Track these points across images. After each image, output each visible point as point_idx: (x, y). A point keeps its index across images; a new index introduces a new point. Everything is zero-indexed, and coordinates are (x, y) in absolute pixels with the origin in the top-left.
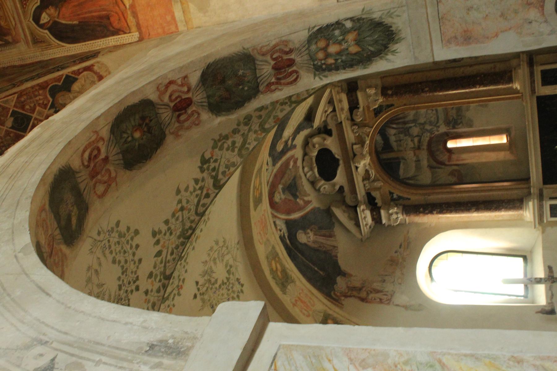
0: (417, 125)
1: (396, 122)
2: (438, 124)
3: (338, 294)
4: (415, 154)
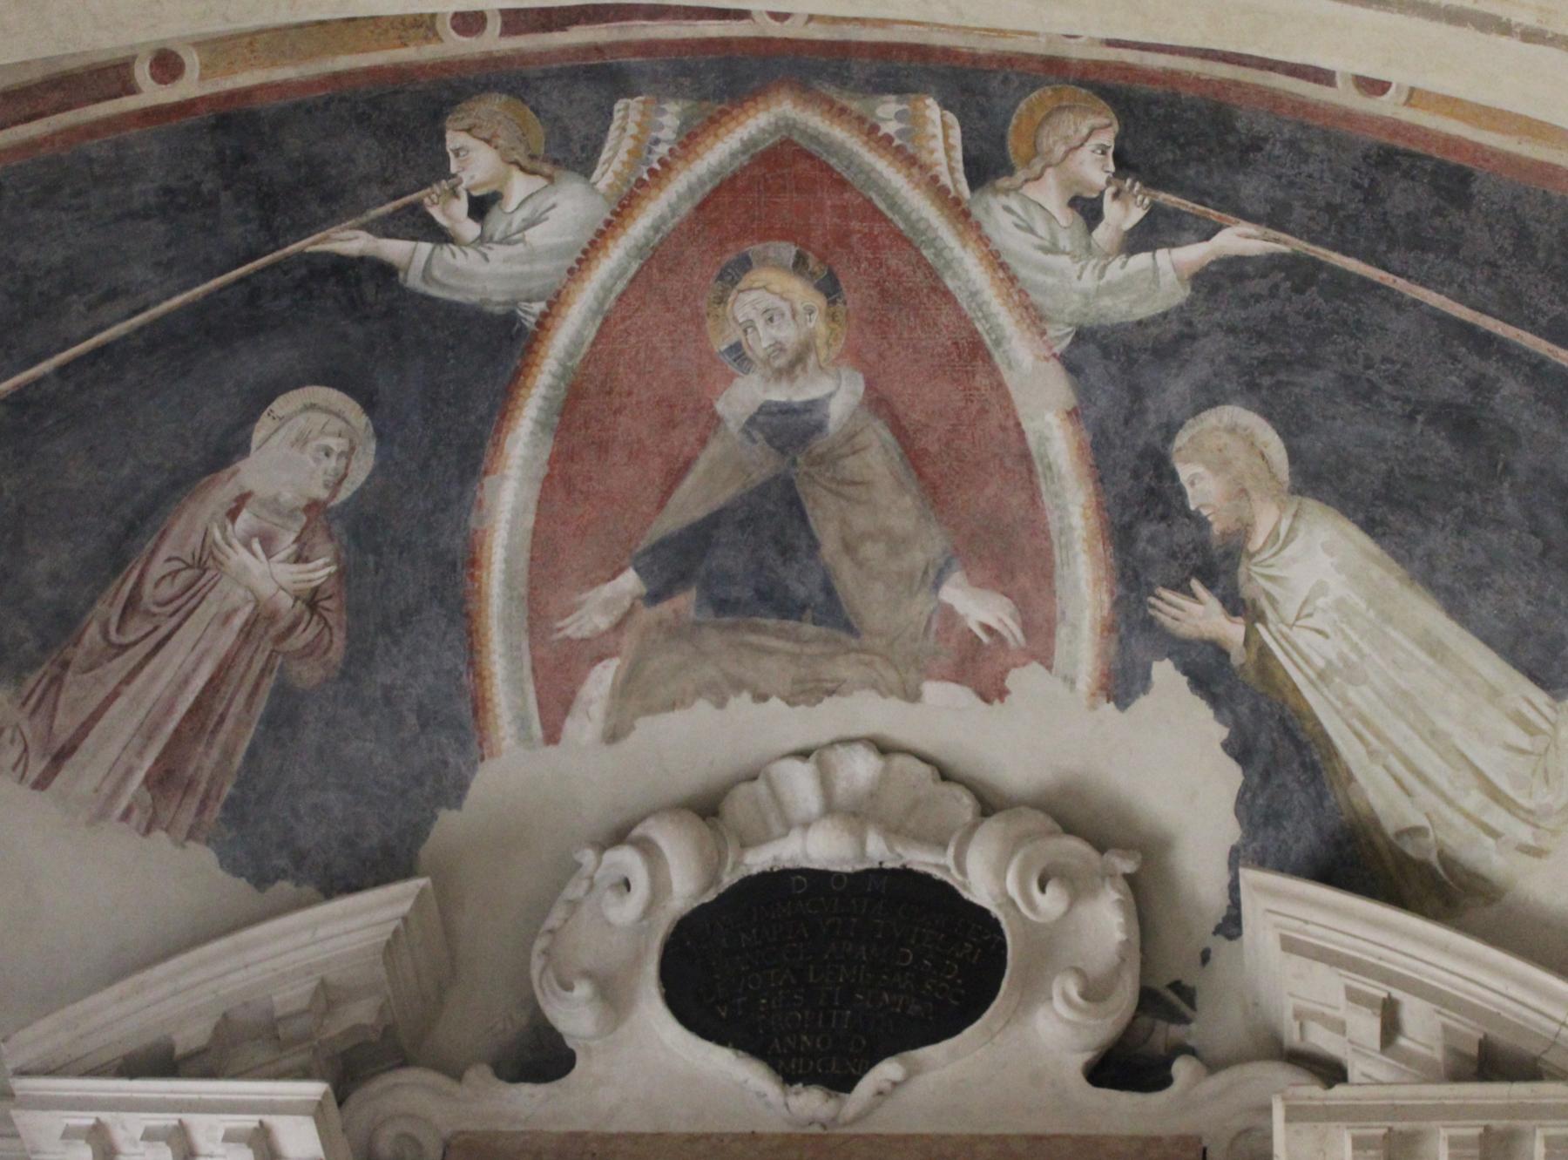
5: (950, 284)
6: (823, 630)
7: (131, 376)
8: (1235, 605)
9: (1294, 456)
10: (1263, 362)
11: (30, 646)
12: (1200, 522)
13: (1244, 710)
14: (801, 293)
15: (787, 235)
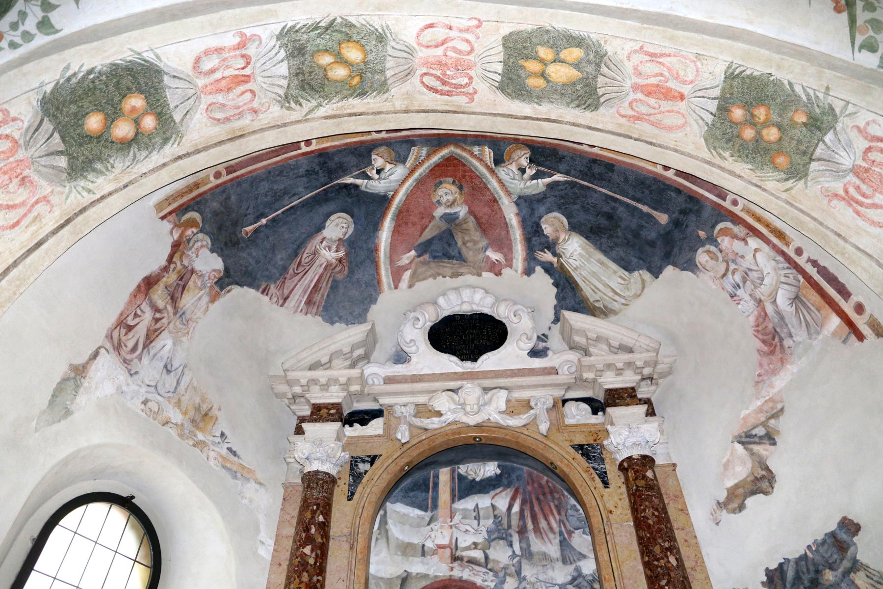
1: (527, 514)
3: (189, 232)
5: (489, 187)
6: (458, 262)
8: (555, 254)
9: (569, 224)
10: (563, 203)
12: (547, 237)
13: (557, 276)
14: (454, 189)
15: (450, 176)
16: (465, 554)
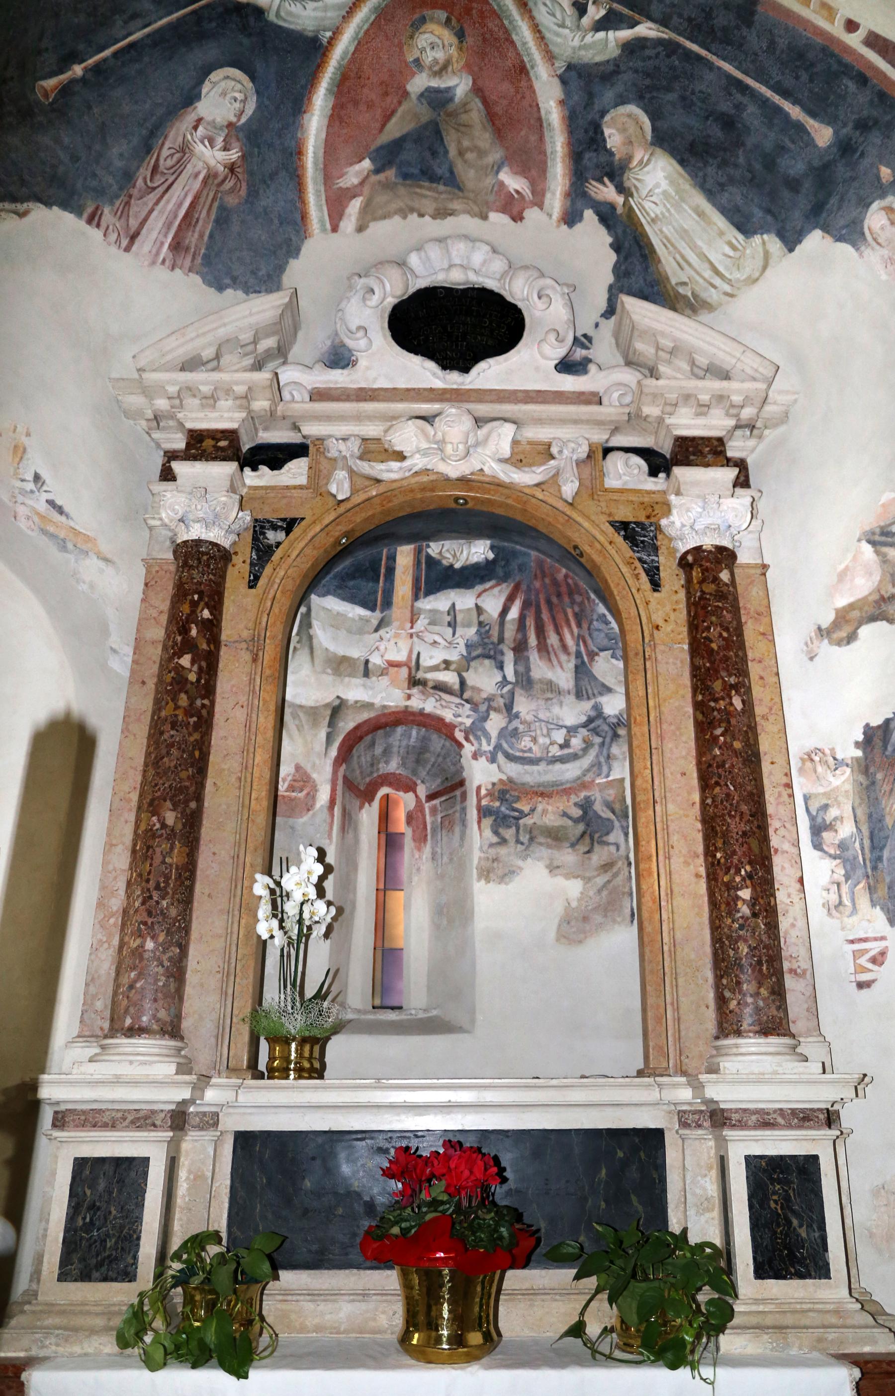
0: (509, 687)
1: (530, 623)
2: (500, 757)
4: (392, 664)
5: (515, 37)
6: (449, 188)
7: (146, 59)
8: (621, 189)
9: (654, 129)
10: (647, 87)
11: (115, 187)
12: (611, 154)
13: (620, 231)
14: (448, 36)
15: (443, 7)
16: (430, 676)
